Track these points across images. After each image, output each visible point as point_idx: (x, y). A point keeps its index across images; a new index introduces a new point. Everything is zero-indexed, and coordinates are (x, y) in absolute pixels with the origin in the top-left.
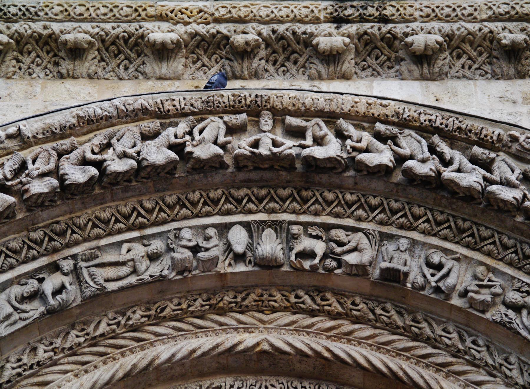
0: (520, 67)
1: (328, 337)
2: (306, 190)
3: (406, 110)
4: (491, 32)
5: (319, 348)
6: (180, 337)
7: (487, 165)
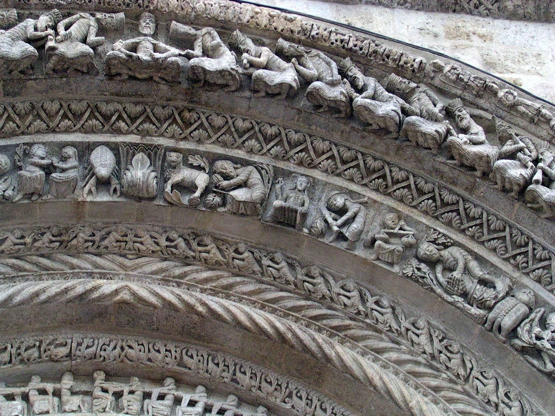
1: (203, 291)
2: (190, 111)
3: (315, 26)
5: (192, 301)
6: (20, 278)
7: (406, 96)
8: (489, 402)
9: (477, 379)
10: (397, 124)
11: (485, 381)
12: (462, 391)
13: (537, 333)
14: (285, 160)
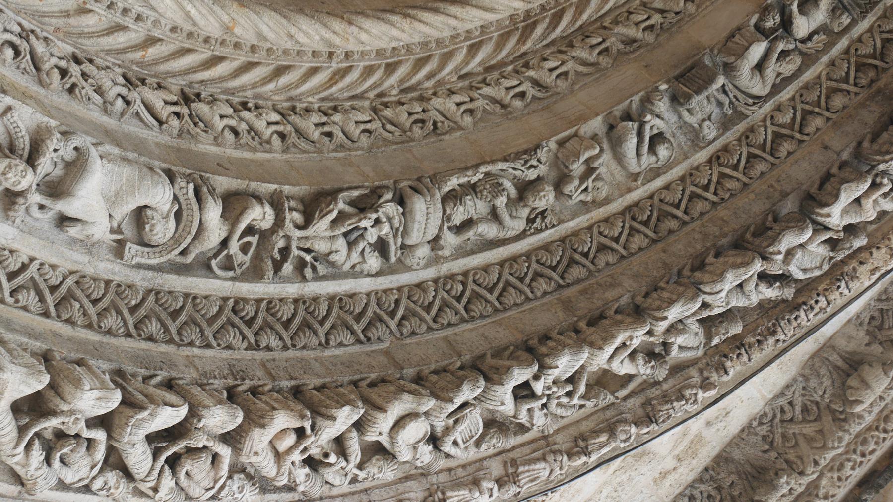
0: (732, 467)
2: (872, 81)
3: (846, 292)
4: (801, 473)
8: (335, 108)
9: (369, 122)
10: (701, 284)
11: (362, 127)
12: (366, 95)
13: (383, 226)
14: (740, 137)
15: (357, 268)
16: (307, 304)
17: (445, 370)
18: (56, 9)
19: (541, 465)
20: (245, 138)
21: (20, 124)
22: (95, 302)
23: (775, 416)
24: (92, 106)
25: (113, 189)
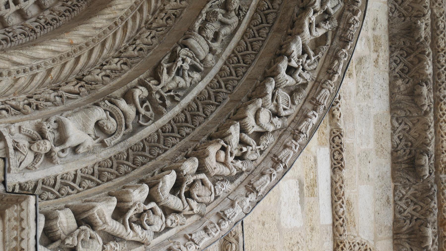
4: (424, 15)
8: (135, 40)
9: (151, 33)
11: (150, 37)
12: (141, 27)
13: (187, 60)
15: (193, 83)
16: (187, 109)
17: (256, 87)
18: (7, 87)
19: (324, 91)
20: (113, 75)
21: (29, 129)
22: (112, 167)
23: (395, 6)
24: (49, 108)
25: (81, 125)
